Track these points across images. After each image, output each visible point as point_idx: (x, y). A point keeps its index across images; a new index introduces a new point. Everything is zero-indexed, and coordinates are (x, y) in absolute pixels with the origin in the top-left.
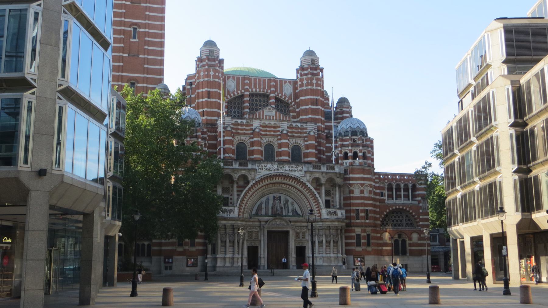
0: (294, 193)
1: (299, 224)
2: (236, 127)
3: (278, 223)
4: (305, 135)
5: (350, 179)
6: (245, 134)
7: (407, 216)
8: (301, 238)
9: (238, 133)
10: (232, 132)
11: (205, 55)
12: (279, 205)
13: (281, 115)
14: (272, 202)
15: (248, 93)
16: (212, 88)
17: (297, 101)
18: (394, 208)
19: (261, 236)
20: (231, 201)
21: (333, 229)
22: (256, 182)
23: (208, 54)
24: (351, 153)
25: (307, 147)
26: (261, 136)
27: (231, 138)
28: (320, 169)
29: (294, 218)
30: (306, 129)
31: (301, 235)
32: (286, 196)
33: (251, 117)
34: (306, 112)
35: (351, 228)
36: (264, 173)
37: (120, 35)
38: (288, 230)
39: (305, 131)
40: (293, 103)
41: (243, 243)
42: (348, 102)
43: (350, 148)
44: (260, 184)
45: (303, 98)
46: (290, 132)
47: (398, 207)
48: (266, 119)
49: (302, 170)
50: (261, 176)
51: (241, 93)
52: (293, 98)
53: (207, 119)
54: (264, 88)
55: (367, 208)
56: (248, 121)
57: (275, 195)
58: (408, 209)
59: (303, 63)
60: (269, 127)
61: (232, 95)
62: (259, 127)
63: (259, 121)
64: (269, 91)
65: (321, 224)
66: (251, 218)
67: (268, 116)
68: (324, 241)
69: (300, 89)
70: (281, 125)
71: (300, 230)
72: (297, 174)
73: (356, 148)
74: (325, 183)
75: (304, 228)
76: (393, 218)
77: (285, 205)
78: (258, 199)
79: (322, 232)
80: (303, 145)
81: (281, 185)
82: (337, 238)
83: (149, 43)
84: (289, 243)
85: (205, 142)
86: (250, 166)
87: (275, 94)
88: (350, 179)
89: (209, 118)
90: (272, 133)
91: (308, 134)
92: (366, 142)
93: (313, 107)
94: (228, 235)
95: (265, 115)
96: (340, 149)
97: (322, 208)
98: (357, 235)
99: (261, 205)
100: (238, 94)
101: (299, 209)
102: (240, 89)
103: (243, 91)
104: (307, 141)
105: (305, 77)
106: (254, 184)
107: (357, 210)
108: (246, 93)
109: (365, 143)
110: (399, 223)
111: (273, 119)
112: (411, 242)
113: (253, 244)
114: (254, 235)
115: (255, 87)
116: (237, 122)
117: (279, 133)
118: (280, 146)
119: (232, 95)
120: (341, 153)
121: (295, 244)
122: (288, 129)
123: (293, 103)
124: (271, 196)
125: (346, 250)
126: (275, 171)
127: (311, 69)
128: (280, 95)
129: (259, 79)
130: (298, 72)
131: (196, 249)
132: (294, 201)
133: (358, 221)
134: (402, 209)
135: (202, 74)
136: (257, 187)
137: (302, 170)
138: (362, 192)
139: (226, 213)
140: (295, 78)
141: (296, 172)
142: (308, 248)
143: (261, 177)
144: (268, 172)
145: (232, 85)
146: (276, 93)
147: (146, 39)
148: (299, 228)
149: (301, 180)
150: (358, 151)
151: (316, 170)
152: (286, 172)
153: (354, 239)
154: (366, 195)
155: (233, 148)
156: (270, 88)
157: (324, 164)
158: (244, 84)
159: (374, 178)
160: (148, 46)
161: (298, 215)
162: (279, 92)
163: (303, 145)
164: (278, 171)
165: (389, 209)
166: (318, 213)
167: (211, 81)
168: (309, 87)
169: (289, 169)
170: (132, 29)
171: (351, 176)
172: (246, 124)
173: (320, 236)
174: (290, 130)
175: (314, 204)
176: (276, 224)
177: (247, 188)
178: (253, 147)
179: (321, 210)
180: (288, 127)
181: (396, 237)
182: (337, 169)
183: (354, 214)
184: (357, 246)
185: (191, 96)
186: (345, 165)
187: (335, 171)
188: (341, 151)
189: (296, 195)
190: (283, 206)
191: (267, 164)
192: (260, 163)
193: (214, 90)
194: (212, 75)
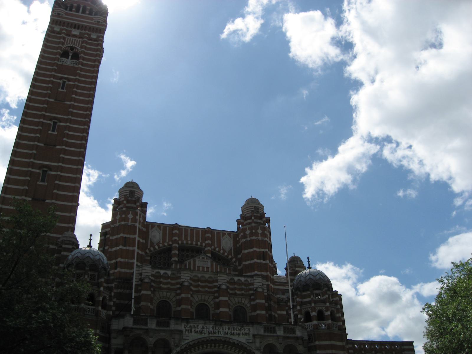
2: (158, 280)
4: (251, 292)
5: (316, 348)
6: (168, 289)
9: (160, 288)
10: (152, 286)
13: (219, 267)
15: (177, 245)
16: (130, 234)
17: (239, 256)
22: (182, 350)
23: (128, 196)
24: (315, 312)
25: (255, 308)
26: (191, 293)
27: (149, 293)
28: (275, 332)
30: (253, 284)
33: (178, 267)
34: (252, 268)
36: (192, 337)
37: (26, 177)
39: (251, 287)
40: (234, 260)
42: (301, 261)
43: (313, 305)
45: (246, 251)
46: (231, 289)
48: (199, 270)
49: (249, 333)
50: (189, 341)
51: (169, 245)
52: (234, 254)
53: (120, 273)
54: (197, 240)
59: (245, 212)
60: (202, 282)
61: (157, 247)
62: (189, 280)
63: (189, 273)
64: (204, 244)
67: (201, 268)
69: (243, 240)
70: (219, 278)
72: (243, 339)
80: (248, 305)
83: (59, 188)
85: (111, 293)
86: (173, 326)
87: (211, 247)
88: (316, 348)
89: (123, 270)
90: (207, 289)
91: (256, 290)
92: (332, 298)
93: (259, 261)
96: (299, 308)
100: (164, 246)
102: (167, 241)
103: (170, 243)
104: (254, 300)
105: (247, 227)
108: (174, 245)
109: (331, 300)
111: (208, 271)
115: (186, 238)
116: (159, 273)
117: (216, 289)
118: (218, 305)
119: (157, 247)
120: (301, 314)
122: (228, 285)
123: (234, 260)
126: (211, 335)
127: (256, 217)
128: (217, 249)
129: (191, 230)
130: (239, 222)
135: (118, 217)
137: (249, 333)
140: (236, 230)
141: (241, 336)
145: (156, 236)
146: (213, 247)
147: (57, 182)
149: (248, 348)
150: (324, 309)
151: (269, 334)
152: (226, 336)
155: (152, 307)
156: (205, 241)
157: (279, 325)
158: (172, 235)
159: (347, 347)
160: (58, 190)
162: (216, 246)
163: (248, 305)
164: (215, 335)
167: (128, 225)
168: (254, 238)
169: (229, 332)
170: (41, 172)
171: (317, 343)
174: (231, 286)
178: (180, 306)
180: (228, 282)
185: (104, 248)
186: (309, 330)
187: (296, 336)
188: (300, 312)
192: (188, 322)
193: (132, 236)
194: (130, 218)
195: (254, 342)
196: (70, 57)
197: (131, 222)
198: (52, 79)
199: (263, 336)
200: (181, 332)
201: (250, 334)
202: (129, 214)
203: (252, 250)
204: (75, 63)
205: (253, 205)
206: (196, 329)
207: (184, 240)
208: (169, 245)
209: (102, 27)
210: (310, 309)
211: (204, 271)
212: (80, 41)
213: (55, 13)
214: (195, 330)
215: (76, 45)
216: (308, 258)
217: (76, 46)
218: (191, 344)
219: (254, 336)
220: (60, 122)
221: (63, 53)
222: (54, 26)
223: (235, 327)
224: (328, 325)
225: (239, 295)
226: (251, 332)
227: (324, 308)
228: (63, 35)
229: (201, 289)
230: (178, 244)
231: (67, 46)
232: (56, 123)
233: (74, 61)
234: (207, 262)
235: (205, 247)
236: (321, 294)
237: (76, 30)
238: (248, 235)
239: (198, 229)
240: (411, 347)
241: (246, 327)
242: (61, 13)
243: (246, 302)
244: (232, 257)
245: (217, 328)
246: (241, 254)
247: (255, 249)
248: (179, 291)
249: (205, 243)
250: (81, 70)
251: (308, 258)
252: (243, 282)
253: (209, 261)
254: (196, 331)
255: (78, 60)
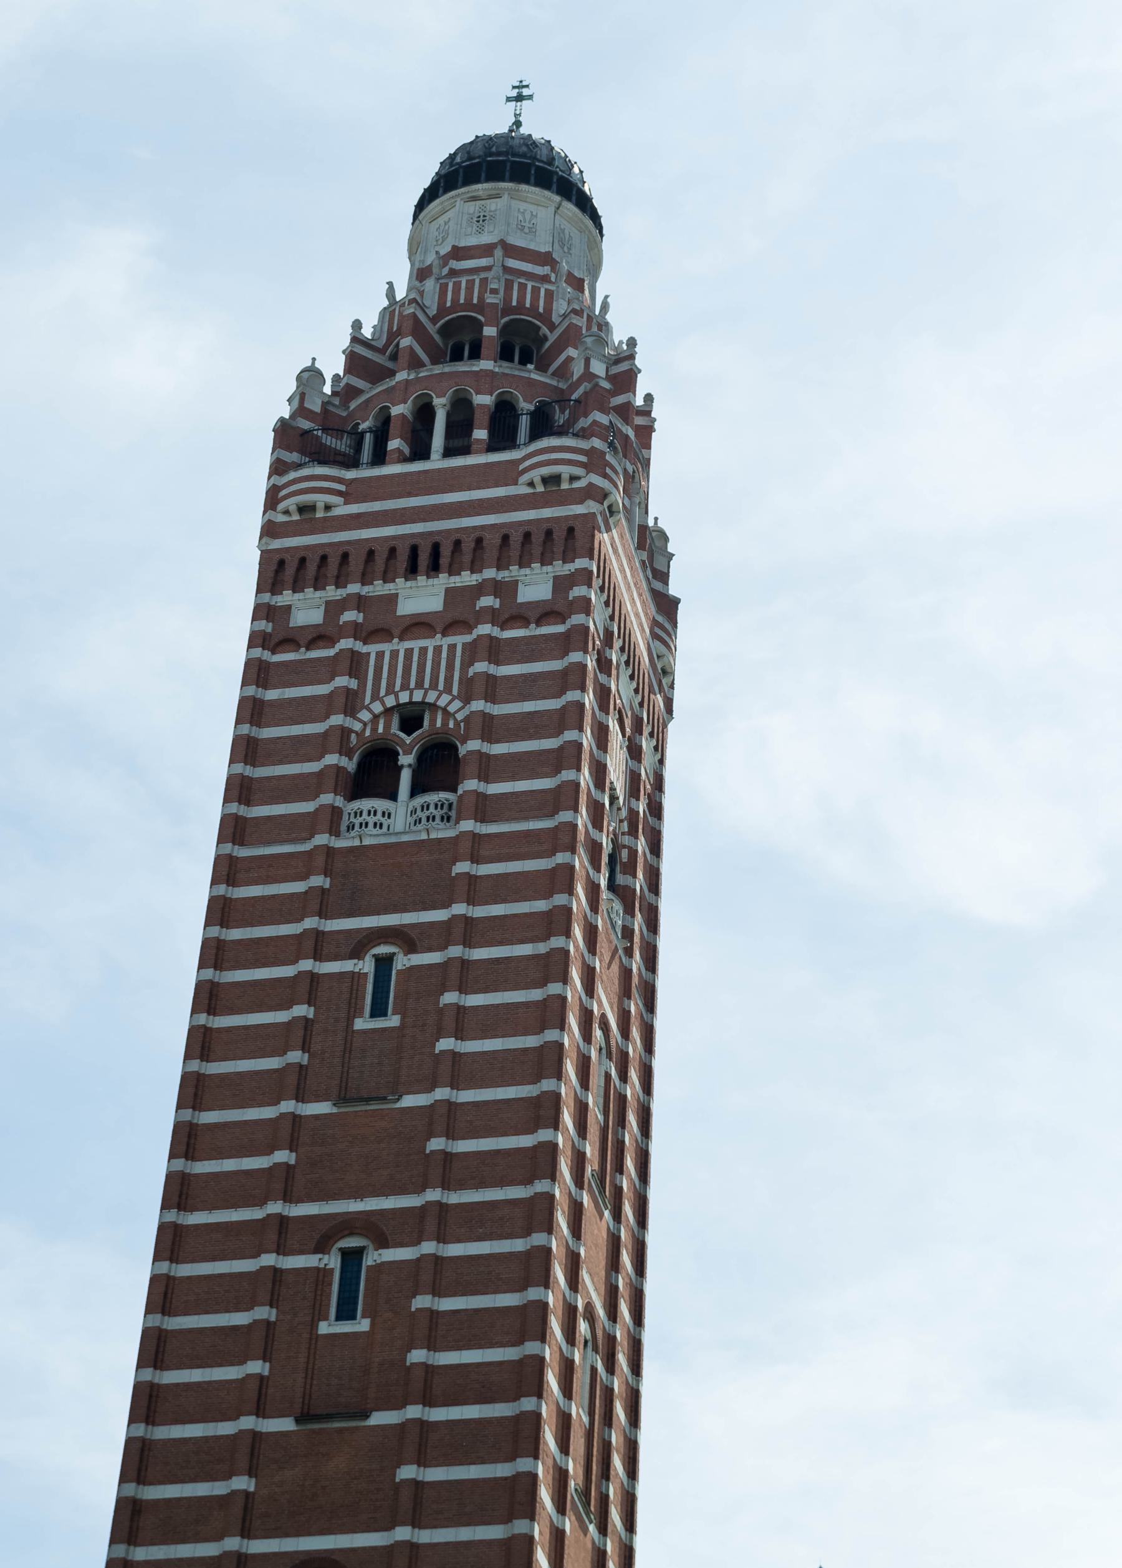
196: (406, 779)
198: (306, 965)
204: (438, 813)
209: (579, 509)
212: (452, 648)
213: (287, 512)
215: (434, 685)
217: (431, 697)
220: (383, 1243)
221: (361, 765)
222: (286, 597)
228: (345, 644)
231: (377, 708)
232: (359, 1252)
233: (433, 798)
237: (422, 579)
242: (321, 499)
250: (477, 847)
255: (454, 790)
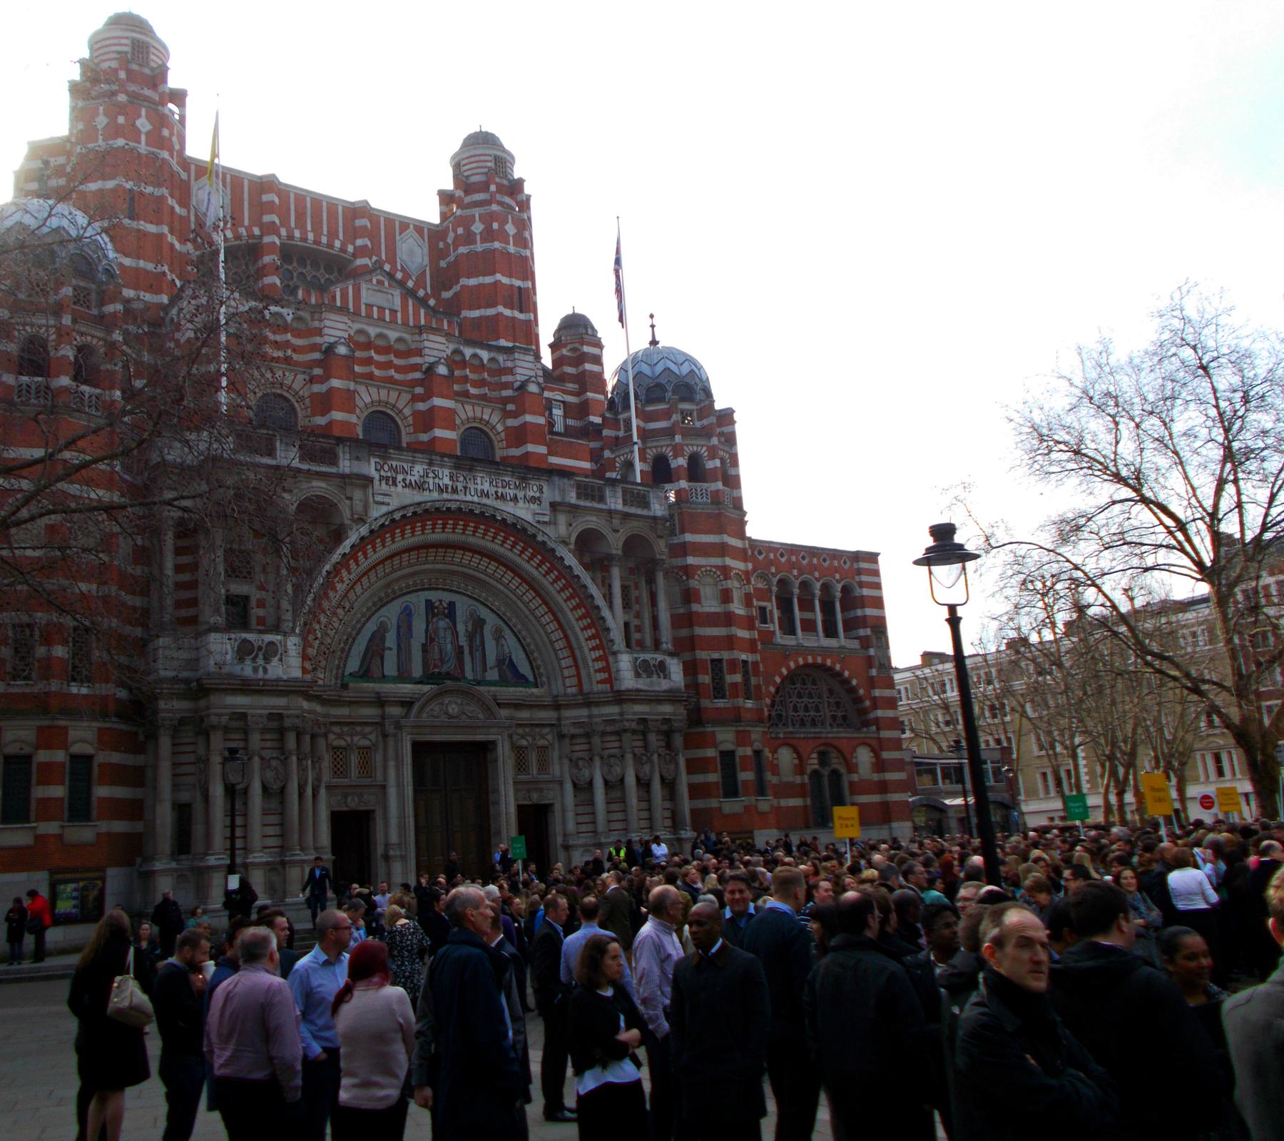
0: (505, 590)
1: (524, 714)
3: (454, 709)
4: (507, 393)
7: (831, 692)
8: (534, 770)
9: (264, 357)
11: (115, 55)
12: (449, 640)
14: (424, 626)
17: (446, 295)
18: (801, 661)
19: (385, 768)
20: (261, 612)
21: (658, 732)
22: (372, 532)
24: (683, 456)
28: (602, 499)
29: (512, 689)
30: (510, 371)
31: (533, 759)
32: (478, 604)
35: (700, 730)
38: (491, 738)
39: (509, 378)
41: (315, 796)
43: (678, 438)
44: (384, 546)
45: (472, 282)
47: (810, 660)
48: (369, 316)
49: (539, 499)
50: (391, 508)
54: (333, 234)
55: (744, 657)
56: (301, 313)
57: (433, 596)
58: (838, 667)
60: (380, 351)
64: (350, 249)
65: (613, 710)
66: (345, 686)
67: (375, 309)
68: (631, 780)
69: (463, 250)
70: (426, 344)
71: (530, 739)
72: (524, 512)
73: (694, 442)
74: (620, 552)
75: (546, 730)
76: (794, 699)
77: (471, 637)
78: (369, 609)
79: (616, 744)
80: (500, 428)
81: (459, 554)
82: (672, 767)
84: (497, 791)
86: (345, 465)
87: (371, 259)
88: (684, 549)
90: (392, 372)
93: (507, 312)
94: (256, 759)
95: (363, 301)
97: (615, 648)
98: (723, 753)
99: (378, 637)
101: (522, 655)
102: (246, 222)
103: (256, 231)
104: (514, 415)
105: (477, 212)
106: (362, 539)
107: (717, 663)
108: (267, 239)
110: (812, 713)
111: (394, 321)
112: (855, 777)
113: (353, 804)
114: (354, 759)
117: (418, 375)
121: (516, 799)
124: (418, 601)
125: (694, 812)
126: (445, 496)
131: (98, 835)
132: (502, 623)
133: (720, 703)
134: (822, 667)
136: (373, 557)
138: (726, 597)
139: (248, 662)
140: (435, 218)
141: (521, 504)
142: (564, 811)
143: (392, 512)
144: (418, 497)
148: (527, 730)
149: (540, 538)
150: (704, 451)
151: (588, 504)
152: (485, 501)
153: (715, 771)
154: (738, 608)
156: (355, 239)
161: (521, 680)
163: (500, 428)
164: (455, 497)
165: (788, 668)
166: (599, 671)
168: (497, 245)
169: (493, 490)
171: (689, 537)
172: (295, 325)
173: (612, 760)
175: (582, 636)
176: (447, 713)
177: (336, 557)
179: (611, 659)
181: (813, 763)
182: (657, 506)
183: (705, 679)
184: (726, 795)
187: (651, 514)
189: (514, 598)
190: (463, 641)
191: (413, 462)
192: (385, 457)
194: (144, 130)
195: (553, 523)
197: (147, 144)
199: (576, 507)
200: (371, 480)
201: (543, 500)
202: (139, 116)
203: (488, 280)
205: (491, 152)
206: (409, 477)
207: (296, 228)
208: (251, 236)
210: (669, 448)
211: (384, 320)
214: (404, 480)
216: (652, 316)
218: (397, 516)
219: (554, 506)
223: (507, 479)
224: (716, 493)
225: (476, 397)
226: (545, 496)
227: (705, 449)
229: (377, 372)
230: (279, 236)
234: (390, 297)
235: (354, 255)
236: (695, 414)
238: (478, 237)
239: (333, 204)
240: (872, 566)
241: (532, 482)
243: (495, 419)
244: (427, 293)
245: (461, 479)
246: (456, 288)
247: (499, 276)
248: (317, 371)
249: (353, 244)
251: (652, 316)
252: (485, 362)
253: (397, 293)
254: (408, 482)
